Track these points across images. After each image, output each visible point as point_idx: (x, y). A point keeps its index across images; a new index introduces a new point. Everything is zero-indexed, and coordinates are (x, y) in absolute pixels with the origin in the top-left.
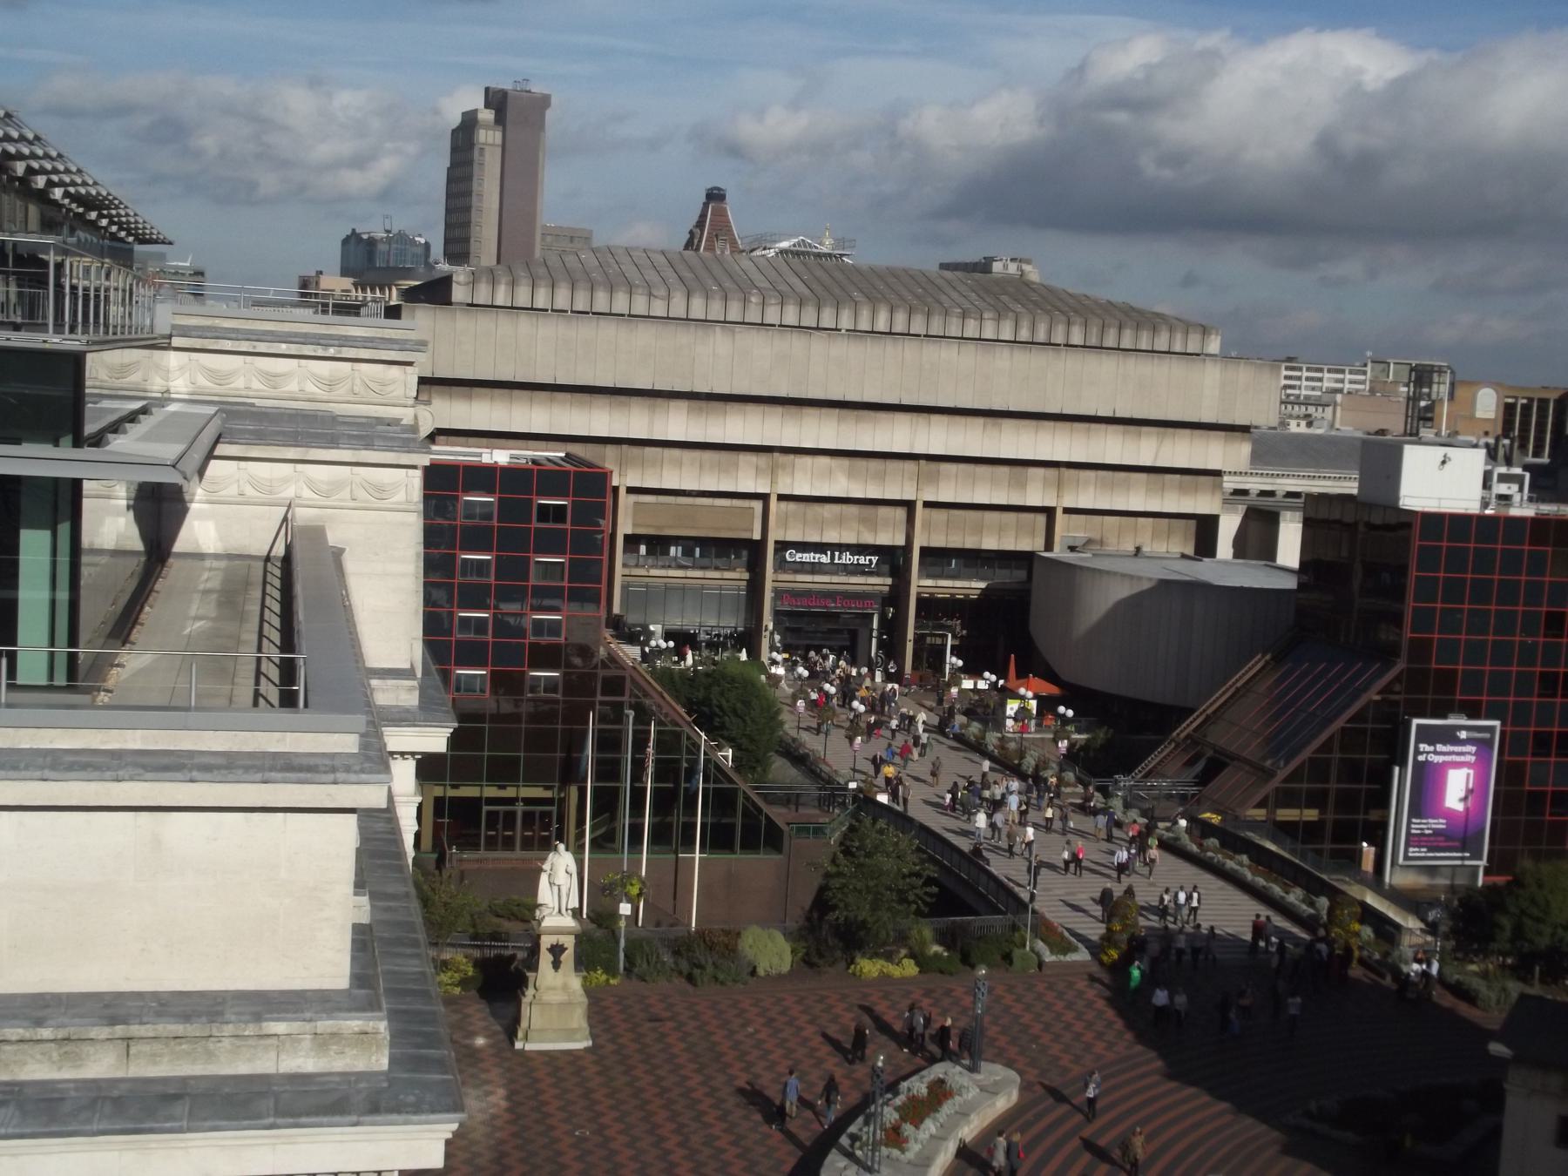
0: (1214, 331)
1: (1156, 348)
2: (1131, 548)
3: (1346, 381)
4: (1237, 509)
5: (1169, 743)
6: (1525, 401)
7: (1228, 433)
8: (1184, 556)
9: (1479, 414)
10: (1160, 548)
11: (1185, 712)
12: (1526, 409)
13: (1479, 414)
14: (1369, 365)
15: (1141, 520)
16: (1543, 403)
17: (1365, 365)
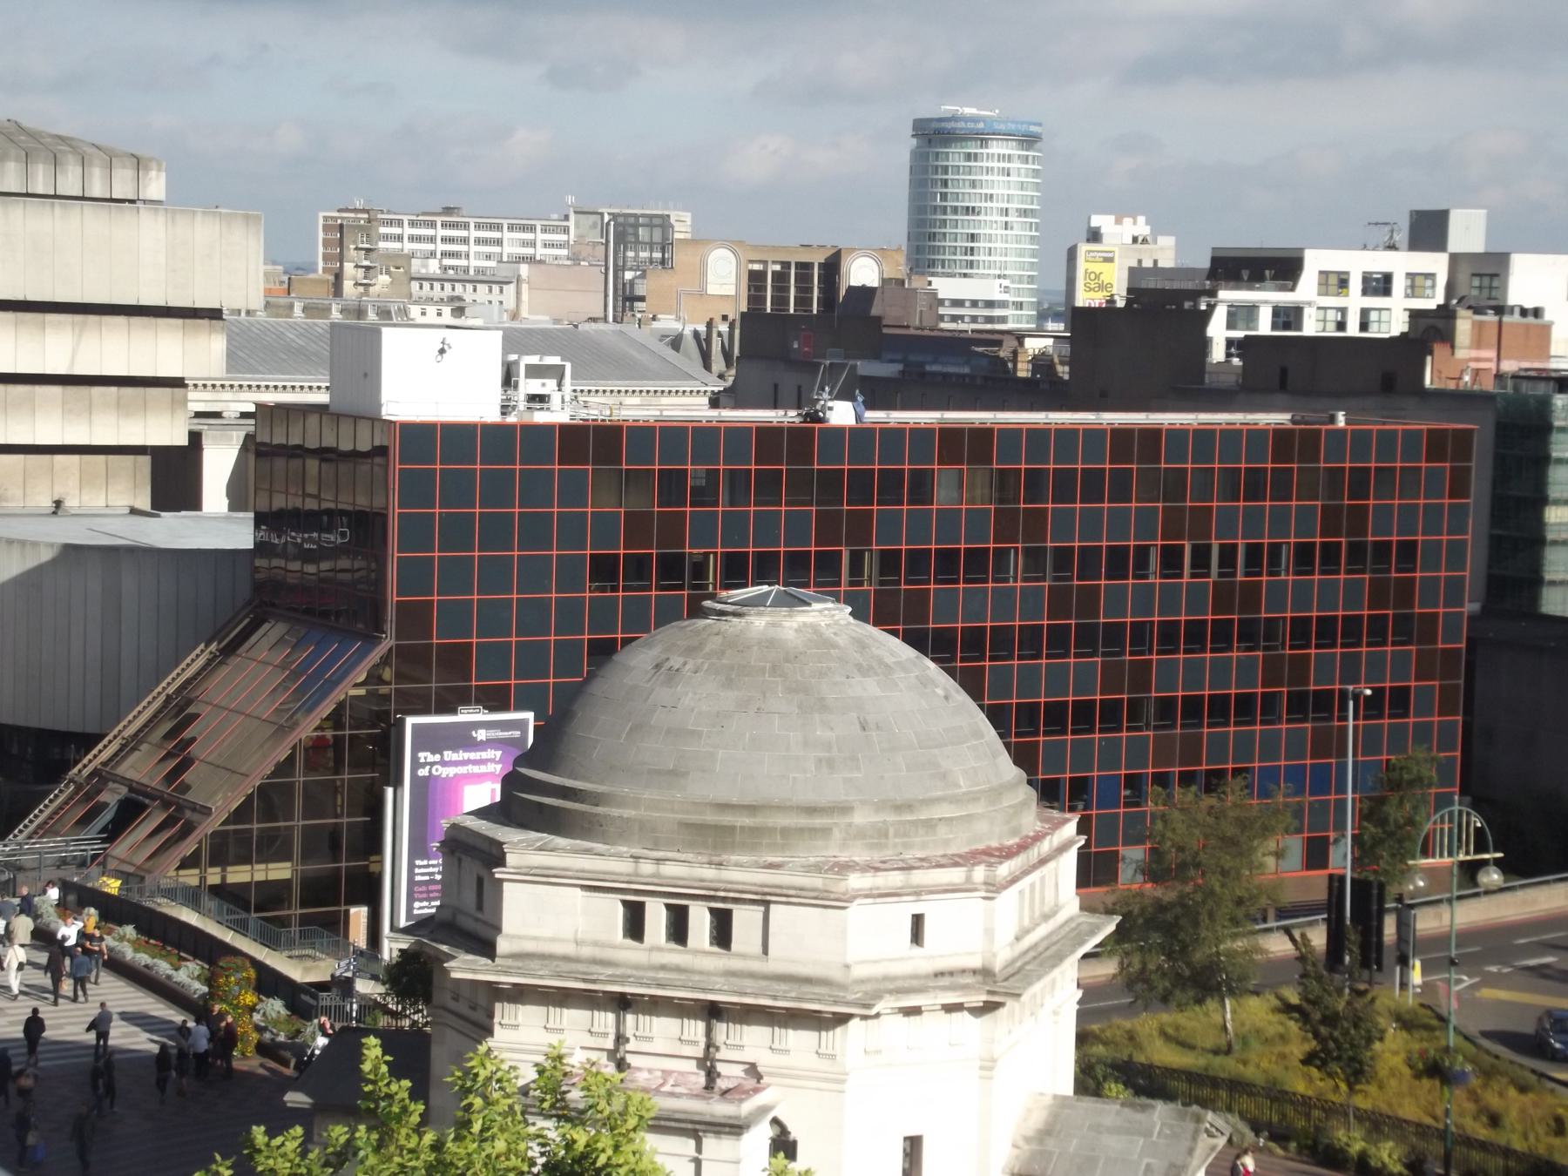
0: (154, 165)
1: (60, 192)
2: (47, 503)
3: (539, 244)
4: (231, 438)
5: (67, 786)
6: (778, 268)
7: (188, 321)
8: (134, 511)
9: (712, 289)
10: (95, 500)
11: (88, 741)
12: (780, 278)
13: (712, 289)
14: (572, 217)
15: (59, 458)
16: (805, 267)
17: (566, 218)
